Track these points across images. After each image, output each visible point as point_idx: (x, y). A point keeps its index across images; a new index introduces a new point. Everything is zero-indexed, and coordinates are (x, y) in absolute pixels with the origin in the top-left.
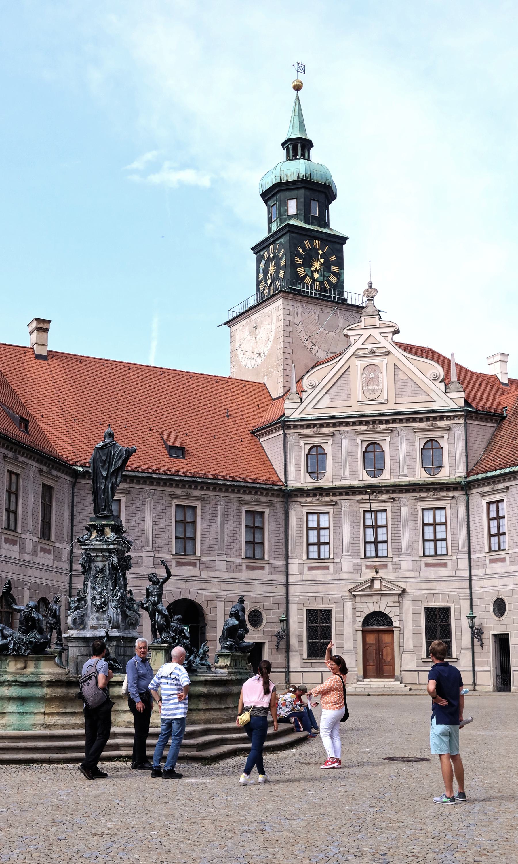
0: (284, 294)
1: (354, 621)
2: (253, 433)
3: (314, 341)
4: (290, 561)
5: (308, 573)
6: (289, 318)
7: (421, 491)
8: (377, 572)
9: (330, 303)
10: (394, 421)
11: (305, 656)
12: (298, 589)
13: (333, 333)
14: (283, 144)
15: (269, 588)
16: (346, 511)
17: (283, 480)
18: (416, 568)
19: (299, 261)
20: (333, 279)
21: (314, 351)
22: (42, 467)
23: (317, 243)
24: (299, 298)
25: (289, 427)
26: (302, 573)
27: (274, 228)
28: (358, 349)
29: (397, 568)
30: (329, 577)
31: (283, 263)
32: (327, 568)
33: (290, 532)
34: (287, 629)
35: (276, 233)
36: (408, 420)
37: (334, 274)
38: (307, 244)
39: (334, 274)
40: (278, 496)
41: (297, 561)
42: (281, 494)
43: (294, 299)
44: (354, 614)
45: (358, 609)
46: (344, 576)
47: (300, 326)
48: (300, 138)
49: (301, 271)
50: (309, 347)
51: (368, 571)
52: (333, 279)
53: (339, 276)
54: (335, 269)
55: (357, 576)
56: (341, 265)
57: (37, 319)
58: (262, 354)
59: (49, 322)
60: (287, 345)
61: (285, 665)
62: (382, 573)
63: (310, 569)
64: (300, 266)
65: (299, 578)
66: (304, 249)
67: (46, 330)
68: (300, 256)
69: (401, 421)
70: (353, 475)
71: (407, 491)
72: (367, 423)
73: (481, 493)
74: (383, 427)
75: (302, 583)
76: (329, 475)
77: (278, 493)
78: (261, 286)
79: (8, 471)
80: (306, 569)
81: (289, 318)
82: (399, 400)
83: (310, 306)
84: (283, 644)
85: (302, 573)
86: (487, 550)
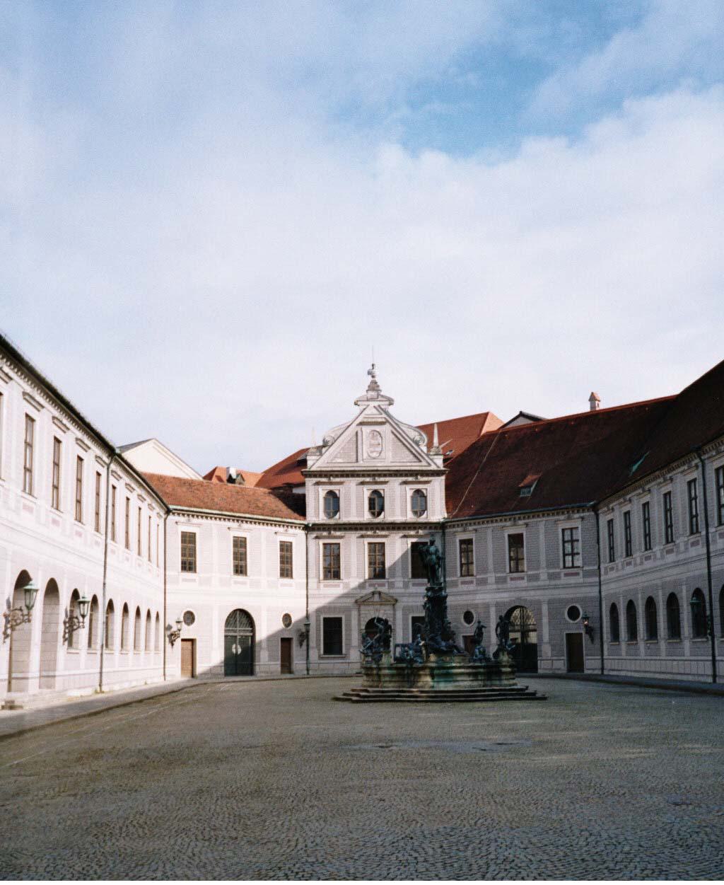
1: (359, 624)
7: (410, 529)
11: (322, 652)
18: (406, 585)
26: (318, 588)
29: (391, 585)
32: (339, 586)
34: (308, 631)
44: (359, 620)
45: (362, 616)
62: (380, 589)
65: (316, 592)
70: (361, 513)
73: (455, 532)
84: (305, 643)
85: (318, 588)
86: (459, 575)
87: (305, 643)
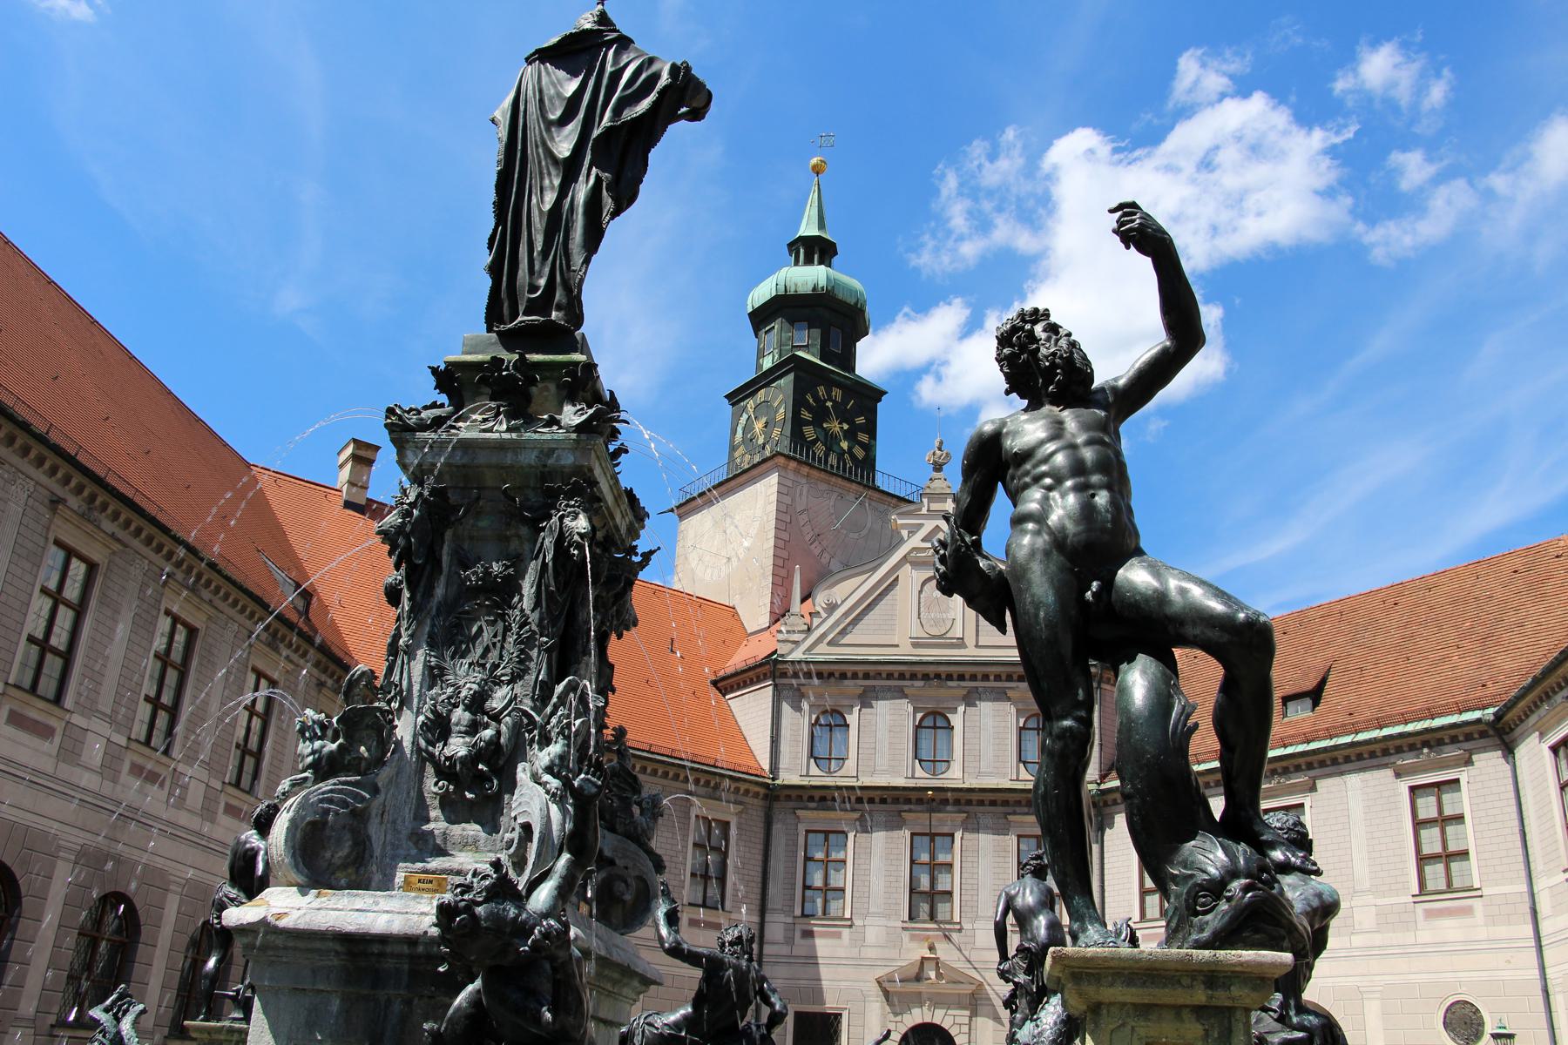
0: (781, 460)
2: (714, 683)
3: (824, 543)
4: (768, 917)
5: (803, 942)
6: (787, 500)
8: (932, 948)
9: (854, 486)
10: (973, 677)
13: (856, 536)
14: (790, 245)
17: (766, 766)
19: (806, 415)
20: (859, 453)
21: (824, 561)
22: (323, 678)
23: (837, 393)
24: (805, 470)
25: (784, 675)
26: (789, 941)
27: (767, 363)
28: (914, 549)
30: (841, 953)
31: (780, 416)
32: (838, 936)
33: (772, 863)
35: (771, 371)
37: (862, 445)
38: (821, 390)
39: (862, 445)
40: (756, 795)
41: (782, 918)
42: (762, 791)
43: (796, 471)
46: (870, 953)
47: (804, 517)
48: (819, 237)
49: (809, 432)
50: (817, 552)
51: (914, 945)
52: (859, 453)
53: (869, 449)
54: (863, 437)
55: (893, 954)
56: (873, 435)
57: (355, 441)
58: (734, 559)
59: (377, 448)
60: (781, 544)
64: (808, 423)
65: (785, 950)
66: (816, 398)
67: (370, 462)
68: (809, 409)
69: (986, 677)
71: (993, 803)
72: (926, 677)
74: (950, 683)
76: (850, 764)
77: (757, 789)
78: (737, 454)
79: (254, 670)
80: (798, 934)
81: (787, 500)
83: (823, 486)
85: (789, 941)
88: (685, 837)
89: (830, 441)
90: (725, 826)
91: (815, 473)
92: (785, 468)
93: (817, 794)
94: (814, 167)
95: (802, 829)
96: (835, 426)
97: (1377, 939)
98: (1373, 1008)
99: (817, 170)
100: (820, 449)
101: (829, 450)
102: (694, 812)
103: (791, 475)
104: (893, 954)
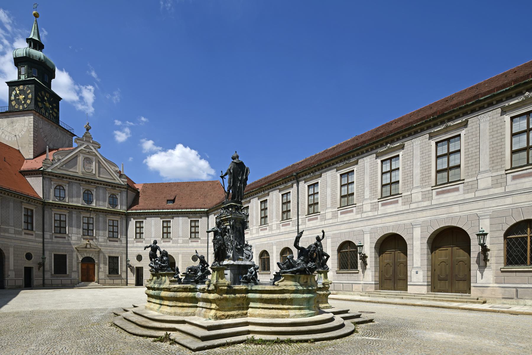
10: (98, 184)
12: (50, 245)
15: (35, 244)
16: (74, 216)
19: (39, 99)
36: (104, 185)
41: (49, 233)
49: (40, 104)
50: (46, 140)
61: (42, 276)
63: (56, 237)
64: (39, 102)
65: (50, 240)
68: (40, 97)
69: (101, 184)
75: (52, 243)
80: (54, 237)
82: (101, 176)
83: (46, 122)
84: (41, 268)
87: (41, 268)
88: (22, 212)
89: (46, 109)
90: (32, 211)
91: (44, 118)
92: (35, 114)
93: (57, 205)
94: (34, 14)
95: (53, 213)
96: (47, 105)
97: (182, 245)
98: (180, 256)
99: (36, 16)
100: (43, 111)
101: (46, 111)
102: (23, 207)
103: (37, 117)
104: (79, 242)
